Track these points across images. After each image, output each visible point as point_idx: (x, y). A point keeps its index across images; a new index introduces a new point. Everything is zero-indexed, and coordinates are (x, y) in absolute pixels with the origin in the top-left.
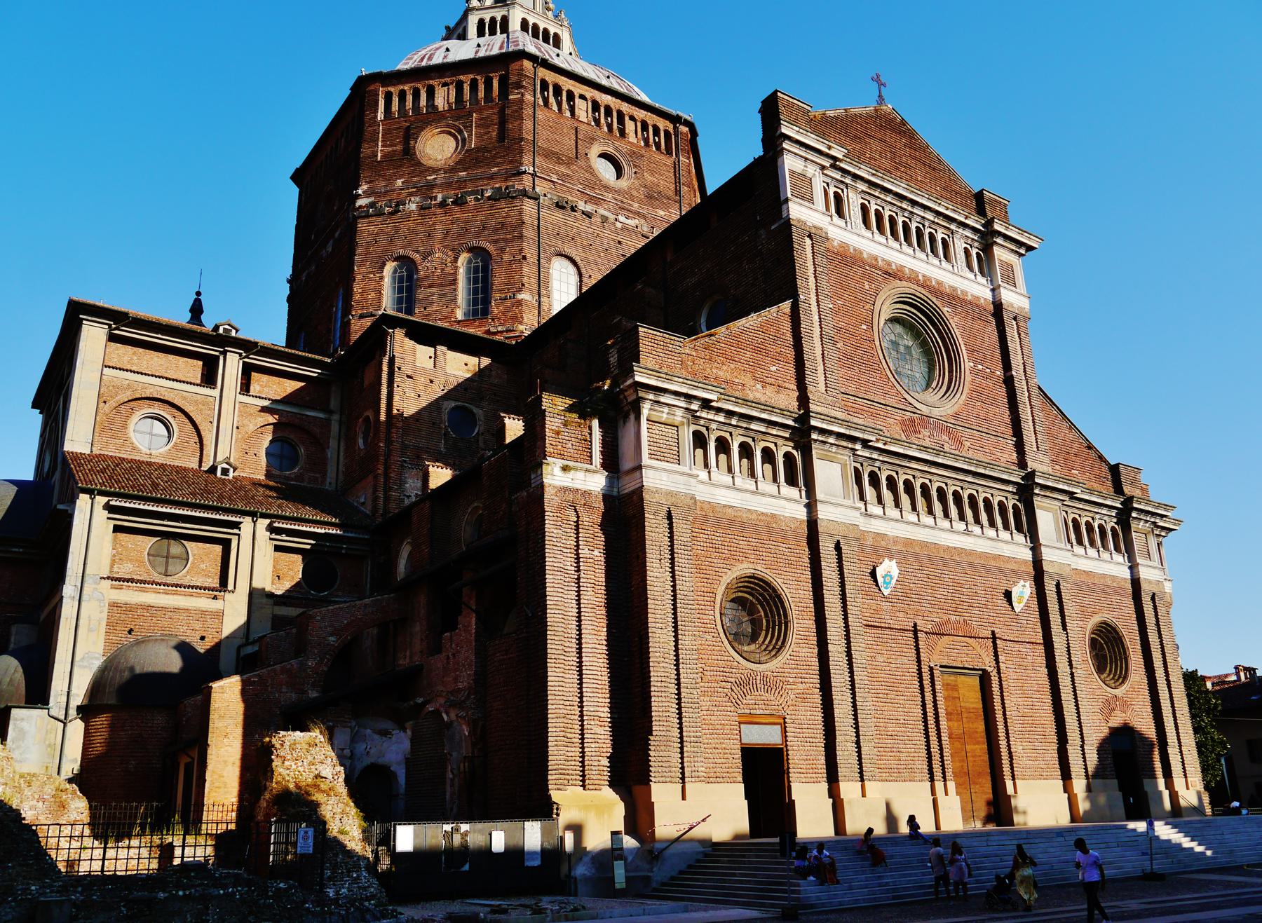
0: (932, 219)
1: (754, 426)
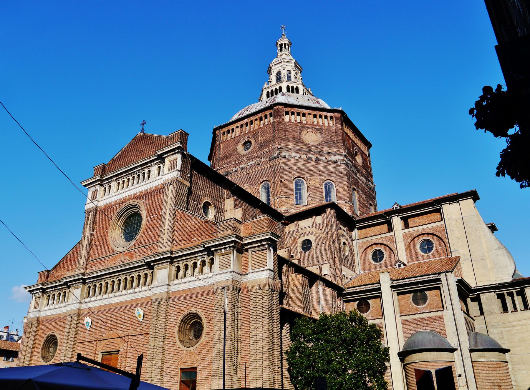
0: (140, 168)
1: (58, 288)
